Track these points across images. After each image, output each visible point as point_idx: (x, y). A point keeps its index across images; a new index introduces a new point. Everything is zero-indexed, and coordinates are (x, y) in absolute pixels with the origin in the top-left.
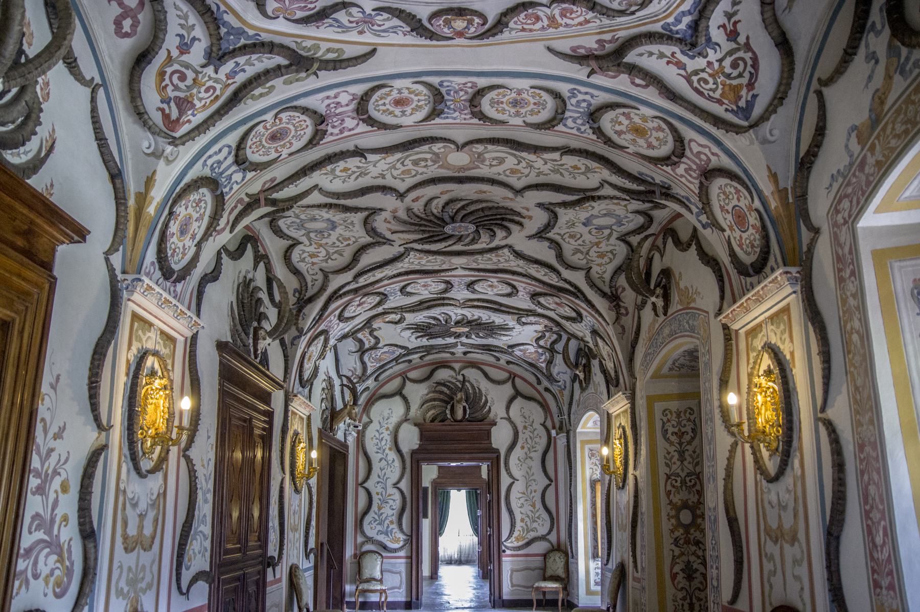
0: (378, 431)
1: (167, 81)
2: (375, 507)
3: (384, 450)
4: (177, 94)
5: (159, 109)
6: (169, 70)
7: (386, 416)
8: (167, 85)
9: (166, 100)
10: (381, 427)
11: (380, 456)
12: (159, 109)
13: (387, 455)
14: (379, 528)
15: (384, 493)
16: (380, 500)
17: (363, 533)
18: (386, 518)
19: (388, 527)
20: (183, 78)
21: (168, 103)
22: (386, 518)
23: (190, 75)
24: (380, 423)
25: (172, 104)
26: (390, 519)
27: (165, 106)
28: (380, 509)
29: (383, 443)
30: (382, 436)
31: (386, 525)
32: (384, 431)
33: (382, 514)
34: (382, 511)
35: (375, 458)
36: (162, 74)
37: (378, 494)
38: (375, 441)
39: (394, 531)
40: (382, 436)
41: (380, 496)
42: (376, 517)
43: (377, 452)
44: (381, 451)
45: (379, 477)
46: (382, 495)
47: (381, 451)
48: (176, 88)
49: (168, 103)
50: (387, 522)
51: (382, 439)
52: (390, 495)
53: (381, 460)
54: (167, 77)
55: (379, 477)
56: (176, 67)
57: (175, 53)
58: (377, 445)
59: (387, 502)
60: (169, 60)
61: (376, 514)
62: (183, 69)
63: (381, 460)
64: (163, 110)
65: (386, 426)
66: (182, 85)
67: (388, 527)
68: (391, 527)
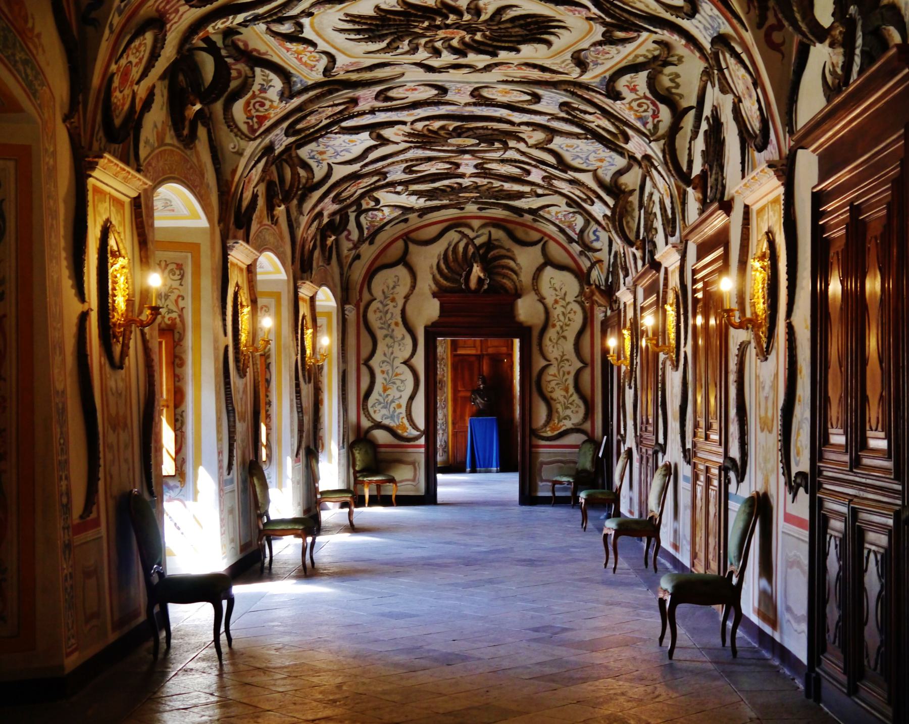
0: (381, 302)
1: (251, 107)
2: (378, 387)
3: (389, 325)
4: (258, 114)
5: (245, 123)
6: (253, 101)
7: (391, 286)
8: (251, 110)
9: (251, 117)
10: (386, 298)
11: (385, 332)
12: (245, 123)
13: (393, 330)
14: (384, 411)
15: (390, 372)
16: (385, 379)
17: (368, 416)
18: (393, 401)
19: (394, 411)
20: (262, 105)
21: (252, 119)
22: (393, 401)
23: (268, 103)
24: (384, 292)
25: (255, 120)
26: (397, 402)
27: (250, 121)
28: (385, 390)
29: (389, 316)
30: (386, 308)
31: (392, 409)
32: (389, 302)
33: (388, 395)
34: (388, 392)
35: (380, 334)
36: (248, 104)
37: (383, 372)
38: (379, 315)
39: (401, 416)
40: (386, 308)
41: (385, 376)
42: (381, 399)
43: (381, 328)
44: (386, 326)
45: (385, 354)
46: (388, 374)
47: (386, 326)
48: (257, 111)
49: (252, 119)
50: (393, 405)
51: (387, 312)
52: (397, 375)
53: (386, 336)
54: (251, 105)
55: (385, 354)
56: (258, 99)
57: (257, 93)
58: (381, 318)
59: (394, 383)
60: (254, 96)
61: (380, 395)
62: (263, 100)
63: (386, 336)
64: (247, 123)
65: (391, 296)
66: (261, 109)
67: (394, 411)
68: (398, 411)
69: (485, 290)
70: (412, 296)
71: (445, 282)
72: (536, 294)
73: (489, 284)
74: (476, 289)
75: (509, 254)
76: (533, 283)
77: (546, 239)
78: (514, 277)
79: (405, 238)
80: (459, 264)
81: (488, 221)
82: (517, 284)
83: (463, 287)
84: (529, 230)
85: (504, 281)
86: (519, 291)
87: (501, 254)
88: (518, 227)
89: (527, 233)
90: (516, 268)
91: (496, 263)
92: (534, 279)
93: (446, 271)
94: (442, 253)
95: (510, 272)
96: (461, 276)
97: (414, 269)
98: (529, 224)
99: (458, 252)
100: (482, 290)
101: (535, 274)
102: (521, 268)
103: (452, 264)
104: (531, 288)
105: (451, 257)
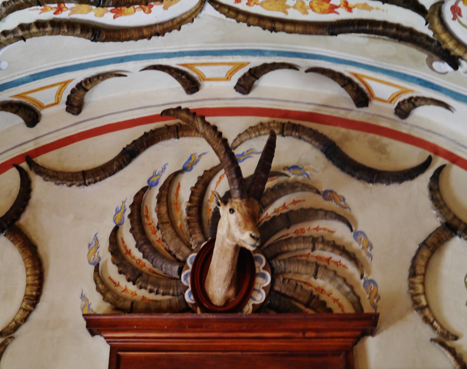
69: (258, 309)
70: (24, 328)
71: (131, 287)
72: (426, 320)
73: (270, 290)
74: (227, 301)
75: (331, 205)
76: (412, 286)
77: (439, 162)
78: (351, 269)
79: (24, 165)
80: (177, 234)
81: (265, 119)
82: (362, 291)
83: (189, 298)
84: (385, 140)
85: (320, 282)
86: (368, 309)
87: (306, 205)
88: (353, 133)
89: (382, 150)
90: (356, 246)
91: (291, 232)
92: (413, 274)
93: (137, 254)
94: (130, 201)
95: (336, 257)
96: (182, 264)
97: (41, 250)
98: (384, 124)
99: (178, 204)
100: (249, 308)
101: (414, 259)
102: (370, 245)
103: (156, 237)
104: (409, 303)
105: (154, 216)
